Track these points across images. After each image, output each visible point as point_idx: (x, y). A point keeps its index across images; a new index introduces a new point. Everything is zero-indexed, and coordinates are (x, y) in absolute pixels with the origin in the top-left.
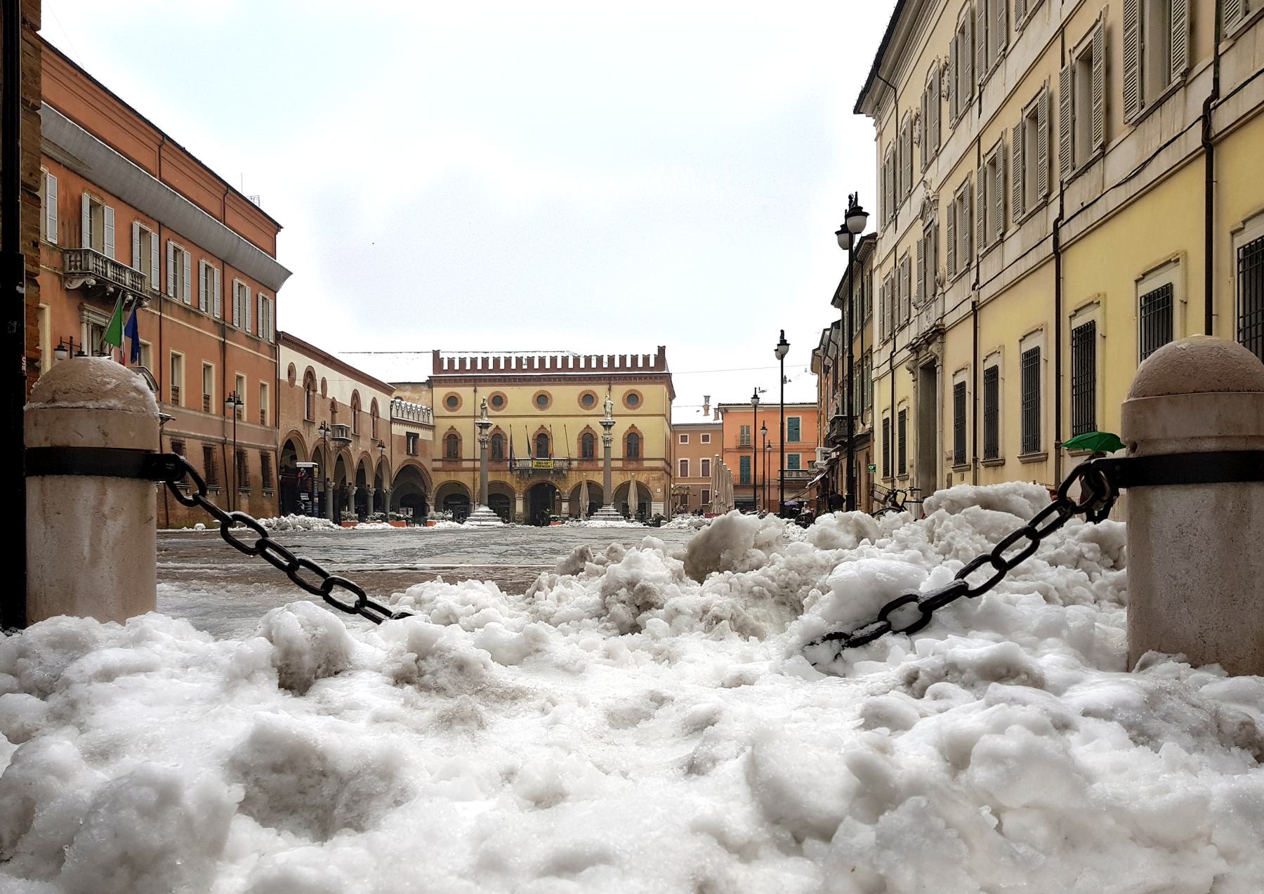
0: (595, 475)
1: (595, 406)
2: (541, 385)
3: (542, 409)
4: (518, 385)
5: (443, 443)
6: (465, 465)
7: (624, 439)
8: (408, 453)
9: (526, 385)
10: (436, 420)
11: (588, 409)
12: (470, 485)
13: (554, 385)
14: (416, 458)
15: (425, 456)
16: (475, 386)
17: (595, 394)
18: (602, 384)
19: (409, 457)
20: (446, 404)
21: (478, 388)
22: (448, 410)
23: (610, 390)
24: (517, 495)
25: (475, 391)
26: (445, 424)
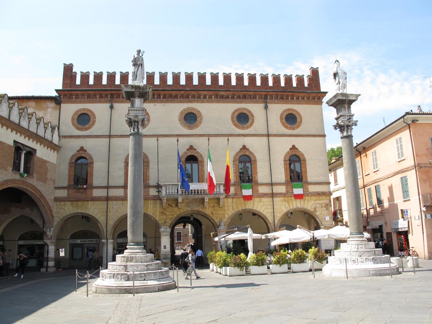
0: (256, 204)
1: (251, 125)
2: (190, 102)
3: (190, 128)
4: (161, 102)
5: (70, 167)
6: (96, 193)
7: (285, 161)
8: (16, 168)
9: (171, 102)
10: (63, 140)
11: (243, 128)
12: (101, 219)
13: (203, 102)
14: (30, 181)
15: (44, 179)
16: (111, 102)
17: (250, 112)
18: (257, 102)
19: (17, 177)
20: (76, 122)
21: (116, 105)
22: (78, 129)
23: (266, 108)
24: (162, 229)
25: (112, 107)
26: (76, 144)
